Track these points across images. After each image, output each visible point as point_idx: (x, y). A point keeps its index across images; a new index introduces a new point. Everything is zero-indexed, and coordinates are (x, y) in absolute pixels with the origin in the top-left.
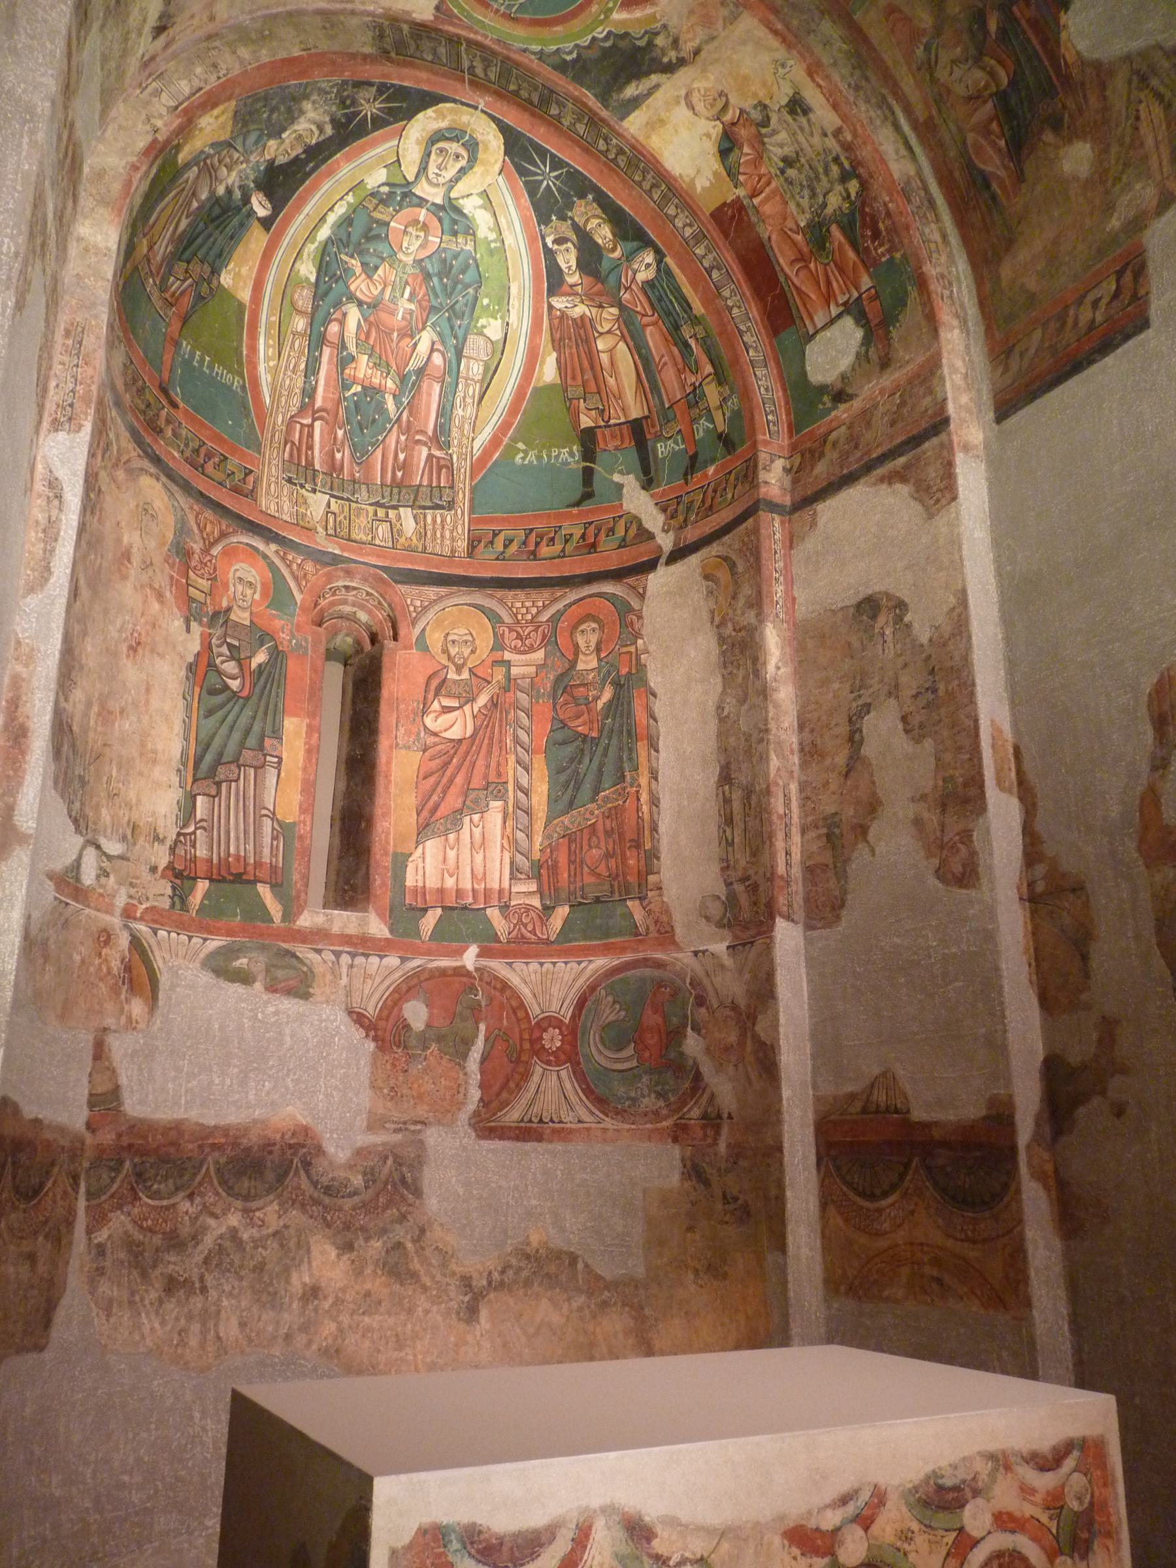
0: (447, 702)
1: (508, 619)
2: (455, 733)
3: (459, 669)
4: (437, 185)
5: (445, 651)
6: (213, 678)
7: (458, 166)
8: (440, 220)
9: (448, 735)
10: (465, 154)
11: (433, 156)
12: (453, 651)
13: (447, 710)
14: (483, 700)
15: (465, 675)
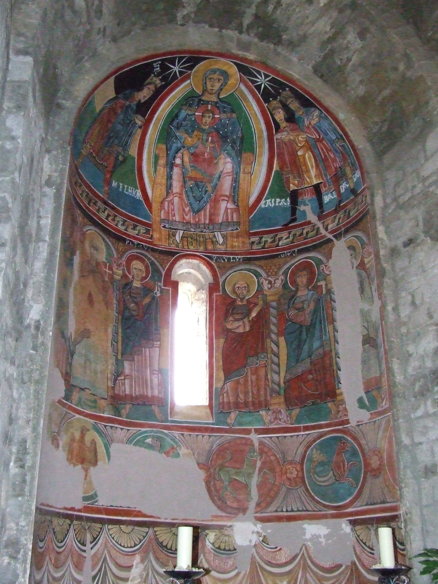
0: (237, 317)
1: (264, 275)
2: (241, 330)
3: (242, 300)
4: (211, 94)
5: (234, 292)
6: (127, 314)
7: (220, 84)
8: (218, 107)
9: (237, 331)
10: (222, 78)
11: (208, 83)
12: (238, 292)
13: (236, 320)
14: (254, 314)
15: (245, 303)
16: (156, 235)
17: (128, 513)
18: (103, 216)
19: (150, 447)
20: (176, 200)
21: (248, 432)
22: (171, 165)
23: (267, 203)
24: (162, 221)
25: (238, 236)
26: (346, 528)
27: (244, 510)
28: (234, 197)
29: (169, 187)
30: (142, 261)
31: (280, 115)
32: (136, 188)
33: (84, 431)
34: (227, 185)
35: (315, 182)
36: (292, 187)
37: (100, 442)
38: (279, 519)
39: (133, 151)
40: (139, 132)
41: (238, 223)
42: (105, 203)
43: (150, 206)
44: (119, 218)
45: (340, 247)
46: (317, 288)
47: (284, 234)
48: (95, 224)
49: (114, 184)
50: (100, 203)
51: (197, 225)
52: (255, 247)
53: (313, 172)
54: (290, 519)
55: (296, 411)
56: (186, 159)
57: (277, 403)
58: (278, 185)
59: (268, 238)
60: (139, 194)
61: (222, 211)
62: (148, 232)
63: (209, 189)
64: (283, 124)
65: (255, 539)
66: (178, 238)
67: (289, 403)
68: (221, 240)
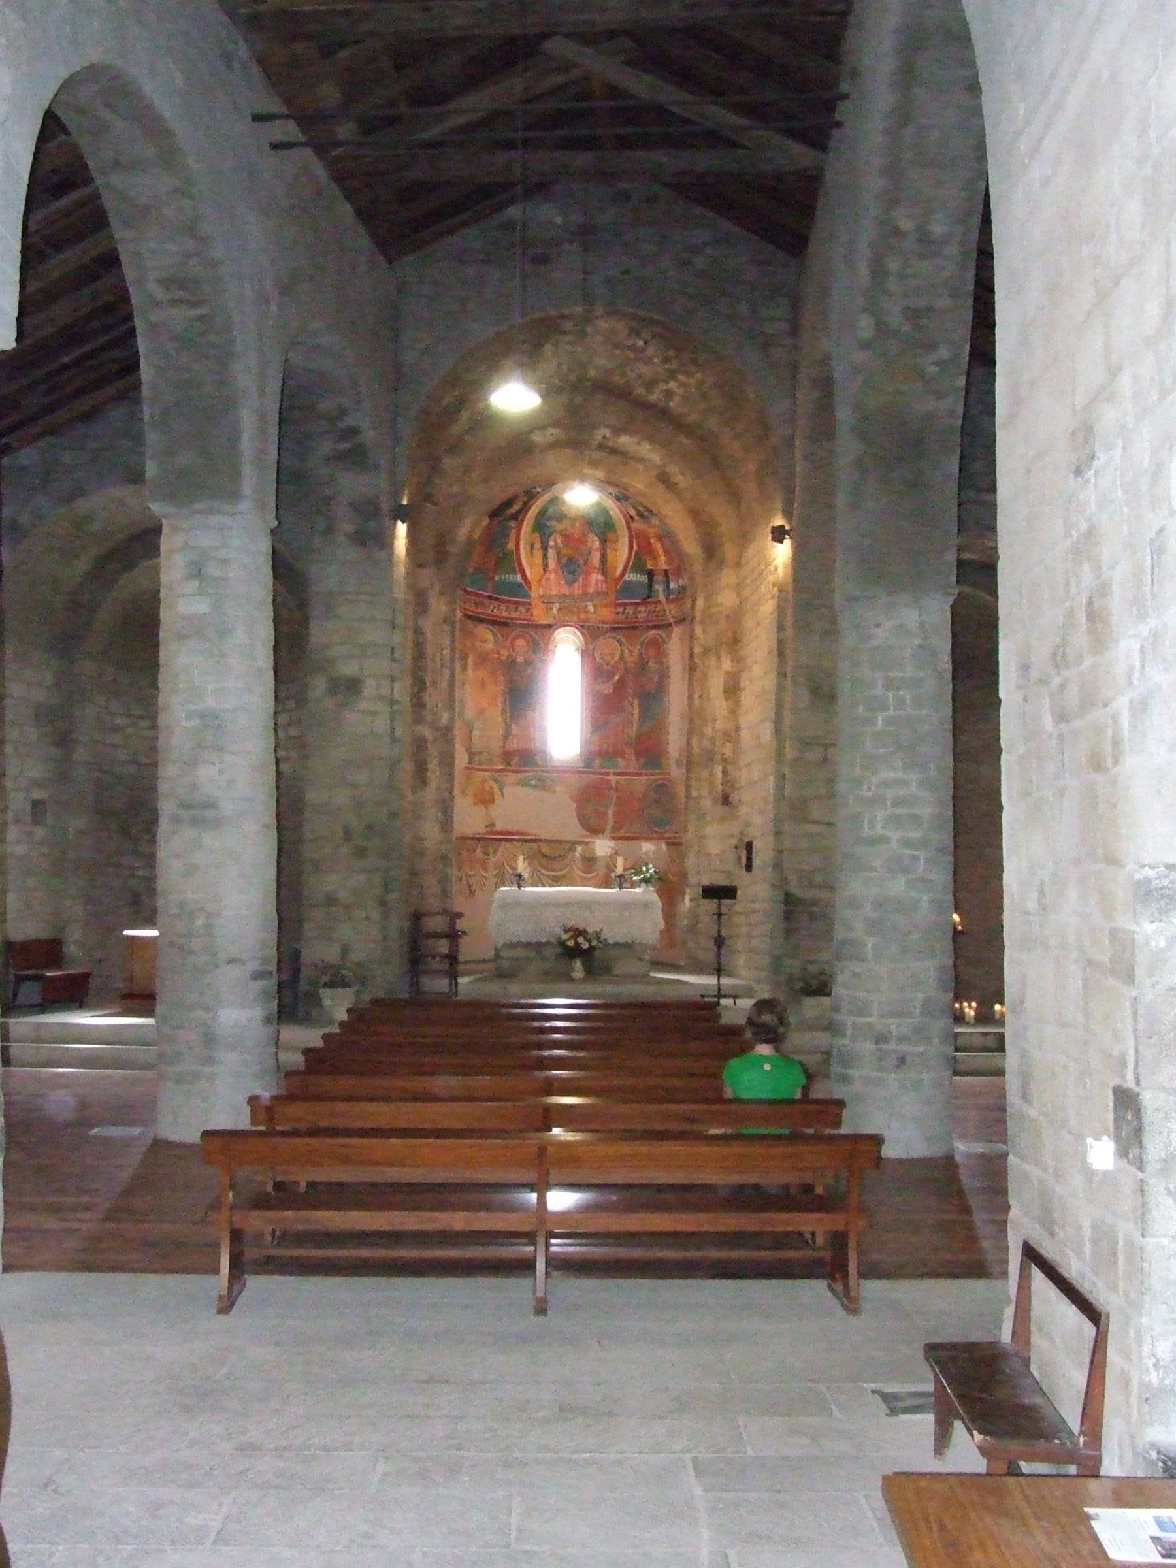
14: (617, 678)
16: (536, 612)
17: (518, 833)
18: (489, 612)
19: (535, 787)
20: (553, 576)
21: (608, 774)
22: (545, 548)
23: (630, 577)
24: (541, 597)
25: (606, 606)
26: (664, 847)
27: (603, 832)
28: (604, 568)
29: (545, 567)
30: (524, 638)
31: (633, 512)
32: (516, 573)
33: (484, 781)
34: (596, 559)
35: (665, 567)
36: (649, 567)
37: (495, 786)
38: (627, 838)
39: (511, 546)
40: (514, 531)
41: (606, 593)
42: (490, 597)
43: (530, 588)
44: (503, 607)
45: (677, 631)
46: (661, 663)
47: (642, 608)
48: (481, 621)
49: (497, 578)
50: (486, 602)
51: (571, 596)
52: (621, 617)
53: (663, 558)
54: (633, 839)
55: (642, 760)
56: (559, 541)
57: (630, 753)
58: (637, 563)
59: (630, 610)
60: (519, 578)
61: (593, 582)
62: (528, 610)
63: (581, 562)
64: (636, 518)
65: (609, 851)
66: (555, 611)
67: (638, 754)
68: (591, 608)
